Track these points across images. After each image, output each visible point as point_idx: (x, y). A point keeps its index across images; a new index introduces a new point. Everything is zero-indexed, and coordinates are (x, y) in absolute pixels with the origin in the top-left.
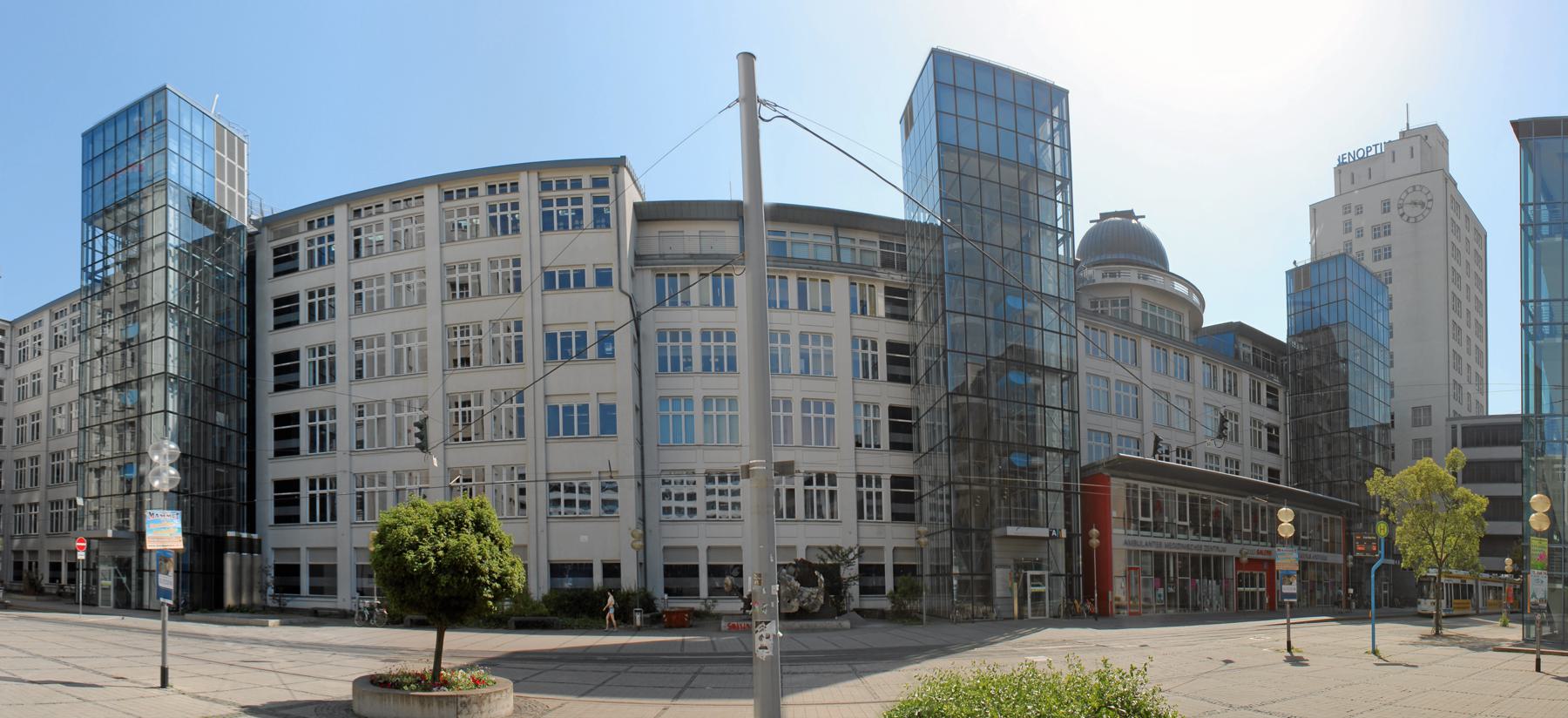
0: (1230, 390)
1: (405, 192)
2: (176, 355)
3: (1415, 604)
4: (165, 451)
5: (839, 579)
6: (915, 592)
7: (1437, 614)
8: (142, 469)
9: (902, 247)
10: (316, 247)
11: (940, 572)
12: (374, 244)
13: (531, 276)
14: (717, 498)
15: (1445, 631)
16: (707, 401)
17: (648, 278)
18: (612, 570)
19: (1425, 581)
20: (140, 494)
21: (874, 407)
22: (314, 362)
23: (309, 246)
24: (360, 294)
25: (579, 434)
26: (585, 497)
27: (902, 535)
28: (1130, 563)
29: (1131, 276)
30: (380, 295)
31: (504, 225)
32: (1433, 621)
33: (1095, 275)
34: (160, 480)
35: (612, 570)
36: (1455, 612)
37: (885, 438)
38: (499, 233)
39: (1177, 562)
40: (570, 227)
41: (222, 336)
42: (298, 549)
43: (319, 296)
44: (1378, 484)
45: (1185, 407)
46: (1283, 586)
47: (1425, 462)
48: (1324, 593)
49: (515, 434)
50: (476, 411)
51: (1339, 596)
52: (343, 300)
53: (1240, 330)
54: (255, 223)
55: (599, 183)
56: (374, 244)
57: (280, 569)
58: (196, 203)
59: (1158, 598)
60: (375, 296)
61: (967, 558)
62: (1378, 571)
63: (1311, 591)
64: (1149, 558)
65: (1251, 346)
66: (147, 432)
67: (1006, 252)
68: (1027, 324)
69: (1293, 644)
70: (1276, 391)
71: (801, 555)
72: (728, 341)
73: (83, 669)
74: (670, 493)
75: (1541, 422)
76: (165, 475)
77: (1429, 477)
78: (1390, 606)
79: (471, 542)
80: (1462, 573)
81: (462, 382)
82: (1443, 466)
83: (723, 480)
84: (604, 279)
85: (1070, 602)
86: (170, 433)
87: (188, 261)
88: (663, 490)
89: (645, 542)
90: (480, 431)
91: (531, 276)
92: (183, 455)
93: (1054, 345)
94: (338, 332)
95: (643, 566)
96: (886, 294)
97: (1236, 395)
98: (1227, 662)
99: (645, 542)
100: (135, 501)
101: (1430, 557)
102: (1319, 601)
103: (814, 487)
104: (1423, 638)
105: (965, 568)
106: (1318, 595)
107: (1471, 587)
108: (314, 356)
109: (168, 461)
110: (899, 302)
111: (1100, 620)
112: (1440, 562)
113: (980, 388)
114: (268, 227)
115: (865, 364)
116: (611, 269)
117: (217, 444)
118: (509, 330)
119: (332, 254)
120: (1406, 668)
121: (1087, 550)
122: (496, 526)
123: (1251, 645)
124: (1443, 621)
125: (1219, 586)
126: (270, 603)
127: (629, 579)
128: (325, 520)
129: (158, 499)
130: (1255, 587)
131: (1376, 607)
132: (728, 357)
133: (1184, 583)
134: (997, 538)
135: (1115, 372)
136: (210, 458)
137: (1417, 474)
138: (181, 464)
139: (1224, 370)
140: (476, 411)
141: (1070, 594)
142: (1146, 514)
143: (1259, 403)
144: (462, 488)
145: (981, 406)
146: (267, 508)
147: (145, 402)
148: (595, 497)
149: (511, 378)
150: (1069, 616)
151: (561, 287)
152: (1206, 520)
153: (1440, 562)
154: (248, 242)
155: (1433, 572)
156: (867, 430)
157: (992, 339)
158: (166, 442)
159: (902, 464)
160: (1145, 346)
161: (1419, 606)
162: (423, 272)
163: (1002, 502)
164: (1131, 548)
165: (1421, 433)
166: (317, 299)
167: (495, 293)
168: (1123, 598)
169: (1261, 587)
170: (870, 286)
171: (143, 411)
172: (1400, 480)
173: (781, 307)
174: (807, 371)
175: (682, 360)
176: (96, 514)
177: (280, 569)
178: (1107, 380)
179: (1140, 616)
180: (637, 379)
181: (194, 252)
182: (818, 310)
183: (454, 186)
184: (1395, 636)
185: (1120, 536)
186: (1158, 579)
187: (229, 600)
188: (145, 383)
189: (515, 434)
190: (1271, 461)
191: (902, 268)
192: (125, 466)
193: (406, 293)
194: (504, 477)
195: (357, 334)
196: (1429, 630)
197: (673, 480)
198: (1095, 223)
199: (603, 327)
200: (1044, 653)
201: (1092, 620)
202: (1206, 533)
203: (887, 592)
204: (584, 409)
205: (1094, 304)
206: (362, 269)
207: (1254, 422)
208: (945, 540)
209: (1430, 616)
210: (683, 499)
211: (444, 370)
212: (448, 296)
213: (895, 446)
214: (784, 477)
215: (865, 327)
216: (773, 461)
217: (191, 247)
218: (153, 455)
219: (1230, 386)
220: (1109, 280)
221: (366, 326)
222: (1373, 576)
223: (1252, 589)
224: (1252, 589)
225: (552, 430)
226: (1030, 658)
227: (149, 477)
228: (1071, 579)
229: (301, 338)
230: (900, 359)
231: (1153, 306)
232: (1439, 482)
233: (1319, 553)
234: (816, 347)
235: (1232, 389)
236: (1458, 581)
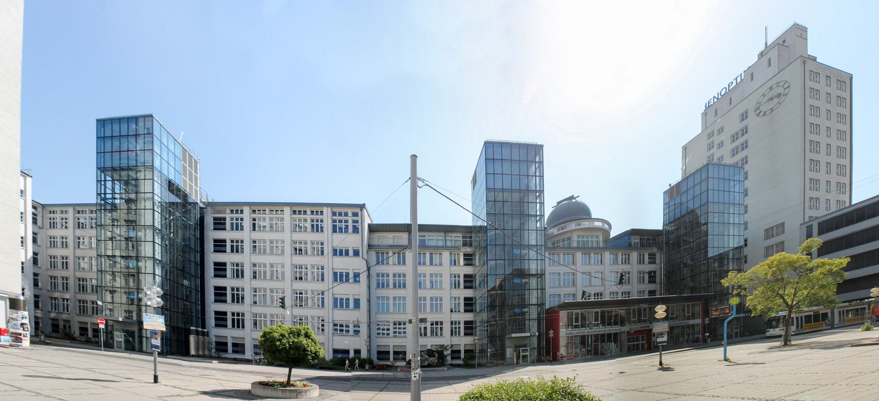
2: (160, 251)
4: (154, 290)
8: (140, 296)
42: (227, 337)
57: (217, 343)
58: (171, 184)
66: (143, 281)
86: (157, 284)
87: (166, 210)
109: (156, 295)
146: (211, 320)
147: (141, 268)
158: (155, 287)
171: (140, 270)
177: (217, 343)
181: (170, 207)
188: (141, 259)
217: (168, 205)
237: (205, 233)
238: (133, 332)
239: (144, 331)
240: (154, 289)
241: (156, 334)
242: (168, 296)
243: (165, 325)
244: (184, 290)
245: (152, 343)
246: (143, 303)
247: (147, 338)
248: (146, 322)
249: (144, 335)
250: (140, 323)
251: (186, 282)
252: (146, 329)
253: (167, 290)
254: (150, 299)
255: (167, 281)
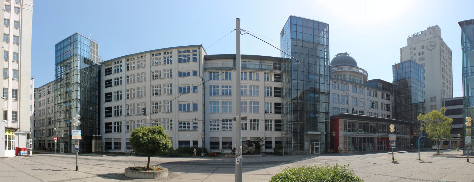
0: (375, 96)
1: (142, 55)
3: (432, 147)
4: (77, 117)
5: (259, 145)
6: (282, 148)
7: (438, 149)
9: (280, 64)
10: (117, 68)
11: (288, 143)
12: (132, 67)
13: (175, 73)
14: (225, 126)
15: (440, 153)
16: (223, 102)
17: (207, 74)
18: (195, 143)
19: (435, 141)
20: (70, 127)
21: (270, 103)
22: (116, 95)
23: (115, 68)
24: (129, 79)
25: (187, 111)
26: (188, 126)
27: (278, 134)
28: (344, 140)
29: (346, 69)
30: (134, 79)
31: (168, 61)
32: (437, 151)
33: (336, 69)
34: (75, 123)
35: (195, 143)
36: (443, 148)
37: (273, 110)
38: (166, 64)
39: (359, 139)
40: (186, 62)
41: (92, 90)
43: (118, 80)
44: (420, 117)
45: (362, 101)
46: (391, 144)
47: (434, 111)
48: (404, 145)
49: (170, 111)
50: (159, 106)
51: (409, 146)
52: (124, 80)
53: (379, 81)
54: (101, 63)
55: (194, 51)
56: (132, 67)
59: (352, 148)
60: (132, 79)
61: (296, 140)
62: (420, 139)
63: (400, 145)
64: (350, 138)
65: (382, 85)
67: (309, 65)
68: (315, 82)
69: (394, 158)
70: (389, 96)
71: (249, 139)
72: (229, 88)
73: (56, 167)
74: (212, 125)
75: (469, 98)
76: (77, 122)
77: (435, 115)
78: (424, 148)
79: (158, 136)
80: (445, 138)
81: (155, 99)
82: (440, 112)
83: (227, 121)
84: (195, 74)
85: (326, 150)
86: (78, 112)
88: (210, 124)
89: (205, 136)
90: (160, 110)
91: (175, 73)
92: (81, 118)
93: (323, 87)
94: (122, 88)
95: (204, 142)
96: (274, 76)
97: (377, 97)
98: (374, 163)
99: (205, 136)
100: (69, 129)
101: (436, 135)
102: (402, 148)
103: (253, 123)
104: (434, 155)
105: (295, 142)
106: (402, 146)
107: (448, 142)
108: (116, 93)
109: (77, 119)
110: (278, 78)
111: (335, 154)
112: (439, 136)
113: (301, 98)
114: (104, 64)
115: (268, 93)
116: (197, 71)
117: (90, 115)
118: (168, 86)
119: (121, 70)
120: (429, 163)
121: (332, 137)
122: (164, 133)
123: (382, 159)
124: (440, 151)
125: (372, 145)
126: (104, 151)
127: (200, 145)
128: (118, 132)
129: (75, 128)
130: (383, 144)
131: (420, 148)
132: (229, 92)
133: (361, 145)
134: (305, 134)
135: (341, 93)
136: (89, 118)
137: (432, 114)
138: (81, 120)
139: (373, 91)
140: (159, 106)
141: (326, 147)
142: (349, 127)
143: (384, 99)
144: (155, 124)
145: (301, 102)
148: (191, 126)
149: (169, 97)
150: (326, 153)
151: (183, 76)
152: (368, 128)
153: (439, 136)
154: (99, 68)
155: (437, 139)
156: (268, 109)
157: (305, 86)
159: (278, 117)
160: (350, 86)
161: (433, 147)
162: (145, 73)
163: (307, 126)
164: (345, 136)
165: (433, 103)
166: (117, 80)
167: (165, 78)
168: (342, 149)
169: (384, 144)
170: (270, 74)
172: (427, 116)
173: (245, 80)
174: (251, 94)
175: (216, 93)
176: (59, 132)
178: (339, 95)
179: (347, 152)
180: (203, 97)
182: (255, 80)
183: (154, 53)
184: (425, 155)
185: (341, 133)
186: (353, 144)
187: (93, 150)
189: (170, 111)
190: (388, 113)
191: (279, 69)
192: (66, 120)
193: (140, 78)
194: (166, 121)
195: (127, 88)
196: (436, 153)
197: (213, 121)
198: (336, 56)
199: (194, 85)
200: (319, 162)
201: (333, 154)
202: (368, 132)
203: (273, 148)
204: (189, 105)
205: (335, 76)
206: (129, 73)
207: (382, 103)
208: (290, 135)
209: (436, 150)
210: (216, 126)
211: (150, 96)
212: (152, 79)
213: (276, 113)
214: (244, 121)
215: (268, 84)
216: (241, 116)
218: (74, 118)
219: (375, 95)
220: (339, 70)
221: (130, 86)
222: (419, 140)
223: (382, 145)
224: (382, 145)
225: (180, 110)
226: (314, 164)
227: (73, 123)
228: (327, 144)
229: (113, 89)
230: (278, 92)
231: (352, 76)
232: (438, 115)
233: (402, 135)
234: (254, 89)
235: (376, 96)
236: (444, 140)
237: (101, 78)
238: (68, 142)
239: (72, 141)
240: (77, 116)
241: (77, 142)
242: (83, 119)
243: (82, 136)
244: (90, 113)
245: (76, 147)
246: (72, 125)
247: (73, 144)
248: (73, 135)
249: (72, 143)
250: (71, 136)
251: (91, 109)
252: (73, 140)
253: (82, 115)
254: (75, 122)
255: (82, 110)
